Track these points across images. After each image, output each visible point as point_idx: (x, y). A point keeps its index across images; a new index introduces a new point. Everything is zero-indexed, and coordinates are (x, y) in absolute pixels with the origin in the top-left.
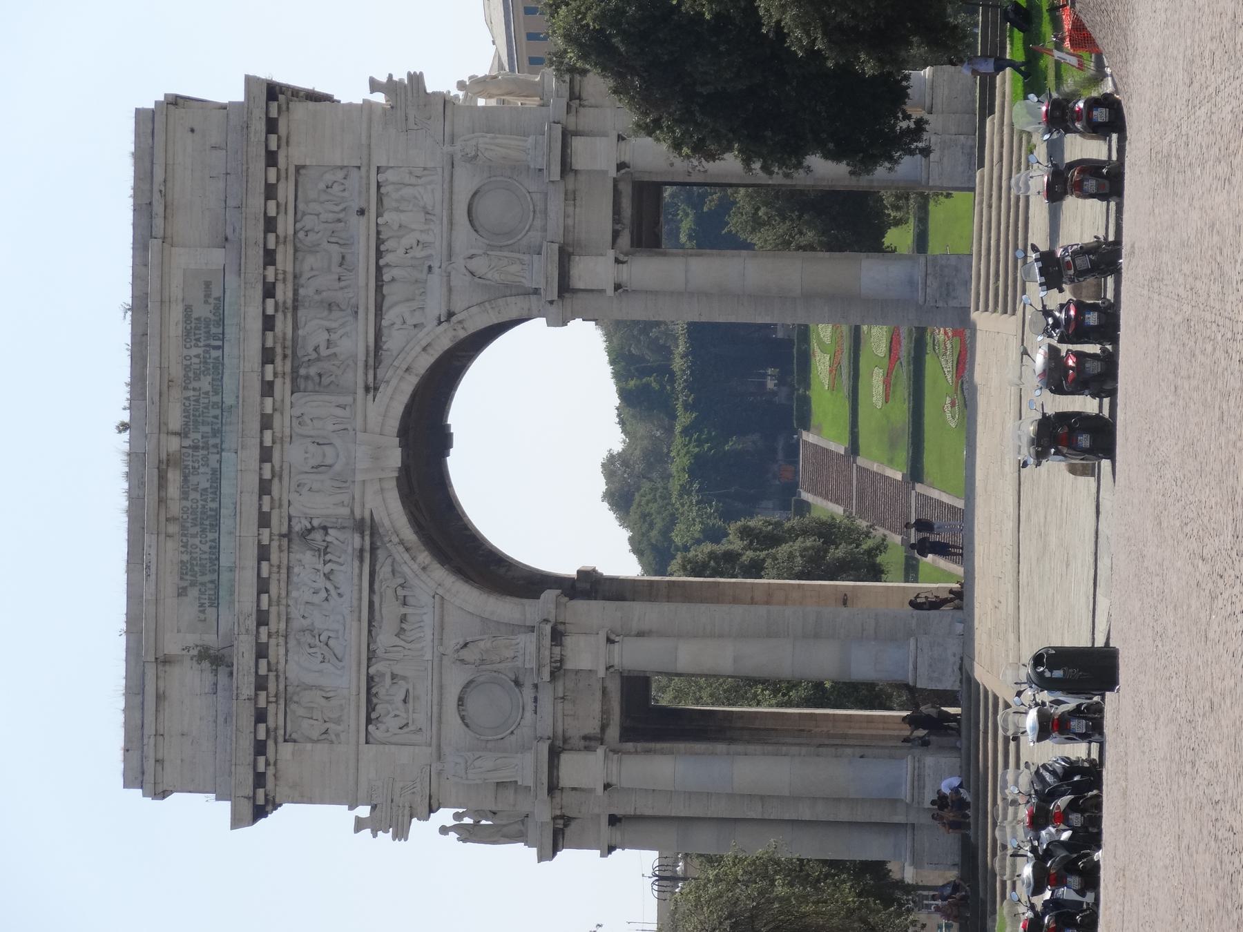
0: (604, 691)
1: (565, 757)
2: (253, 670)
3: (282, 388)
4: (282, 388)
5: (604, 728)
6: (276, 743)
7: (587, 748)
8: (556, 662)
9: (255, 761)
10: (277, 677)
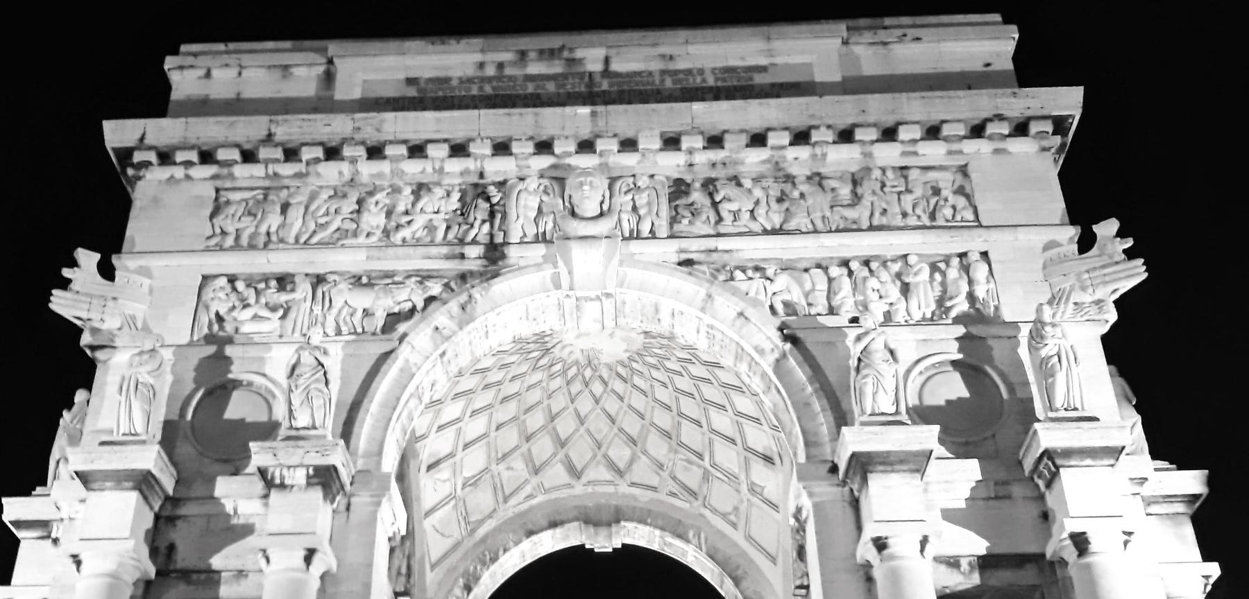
0: (241, 574)
1: (134, 496)
2: (308, 139)
3: (671, 164)
4: (671, 164)
5: (186, 575)
6: (215, 177)
7: (154, 553)
8: (282, 478)
9: (192, 148)
10: (299, 175)
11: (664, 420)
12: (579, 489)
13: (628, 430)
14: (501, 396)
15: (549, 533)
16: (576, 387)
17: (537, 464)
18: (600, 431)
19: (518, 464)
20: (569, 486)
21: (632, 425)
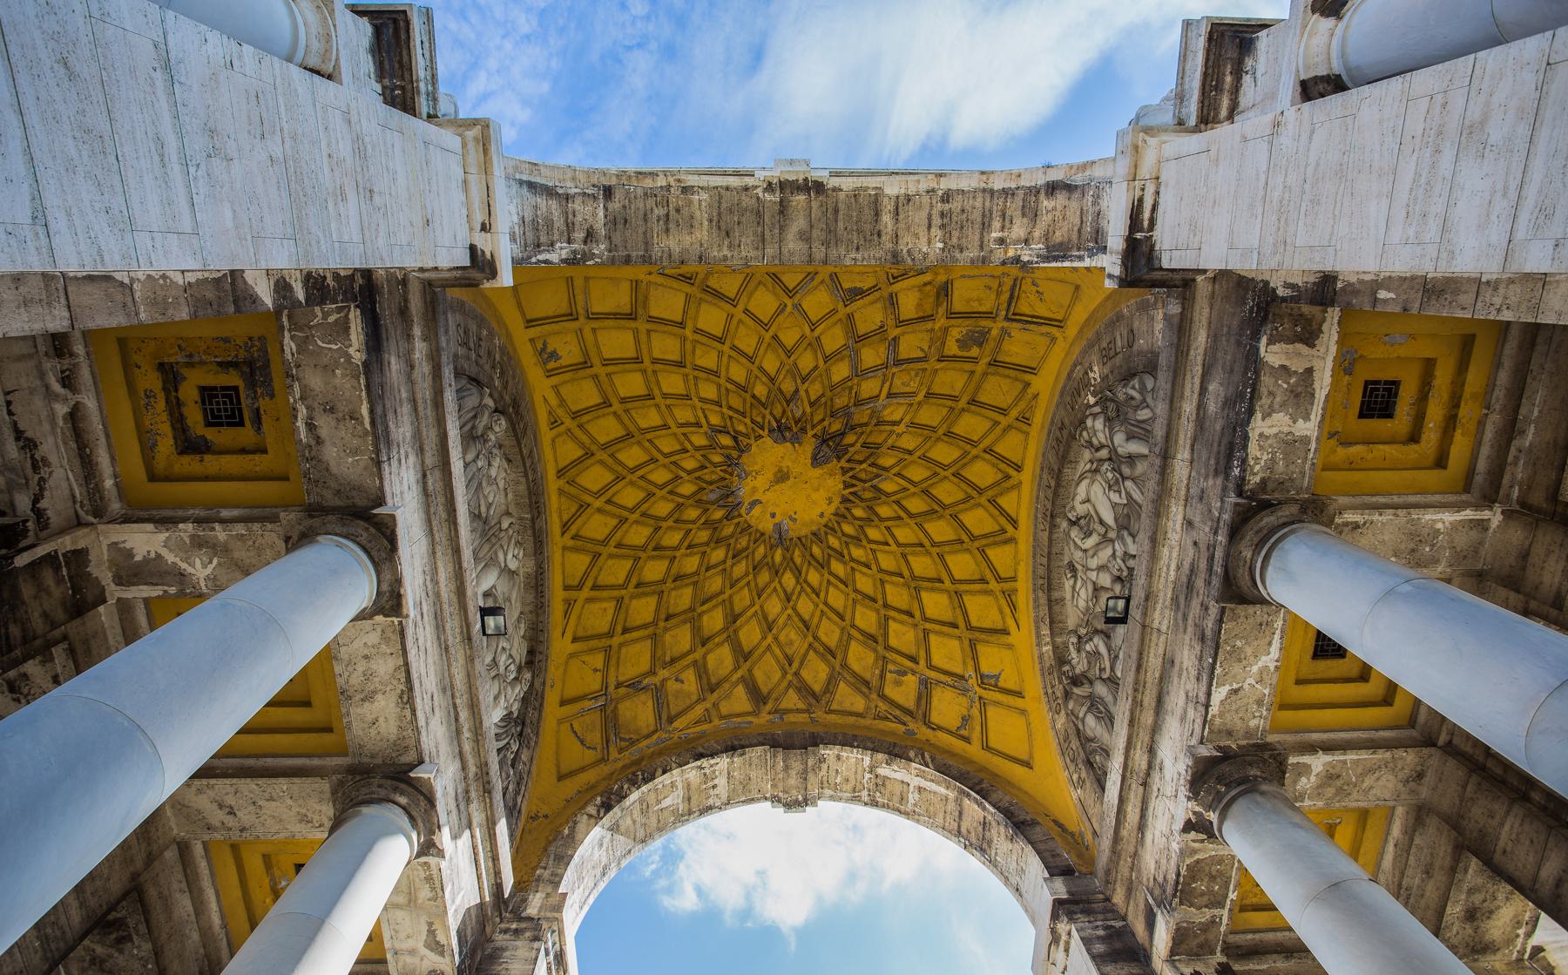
11: (866, 619)
12: (764, 718)
13: (824, 638)
14: (674, 571)
15: (723, 762)
16: (764, 576)
17: (713, 681)
18: (791, 643)
19: (690, 676)
20: (755, 713)
21: (830, 633)
